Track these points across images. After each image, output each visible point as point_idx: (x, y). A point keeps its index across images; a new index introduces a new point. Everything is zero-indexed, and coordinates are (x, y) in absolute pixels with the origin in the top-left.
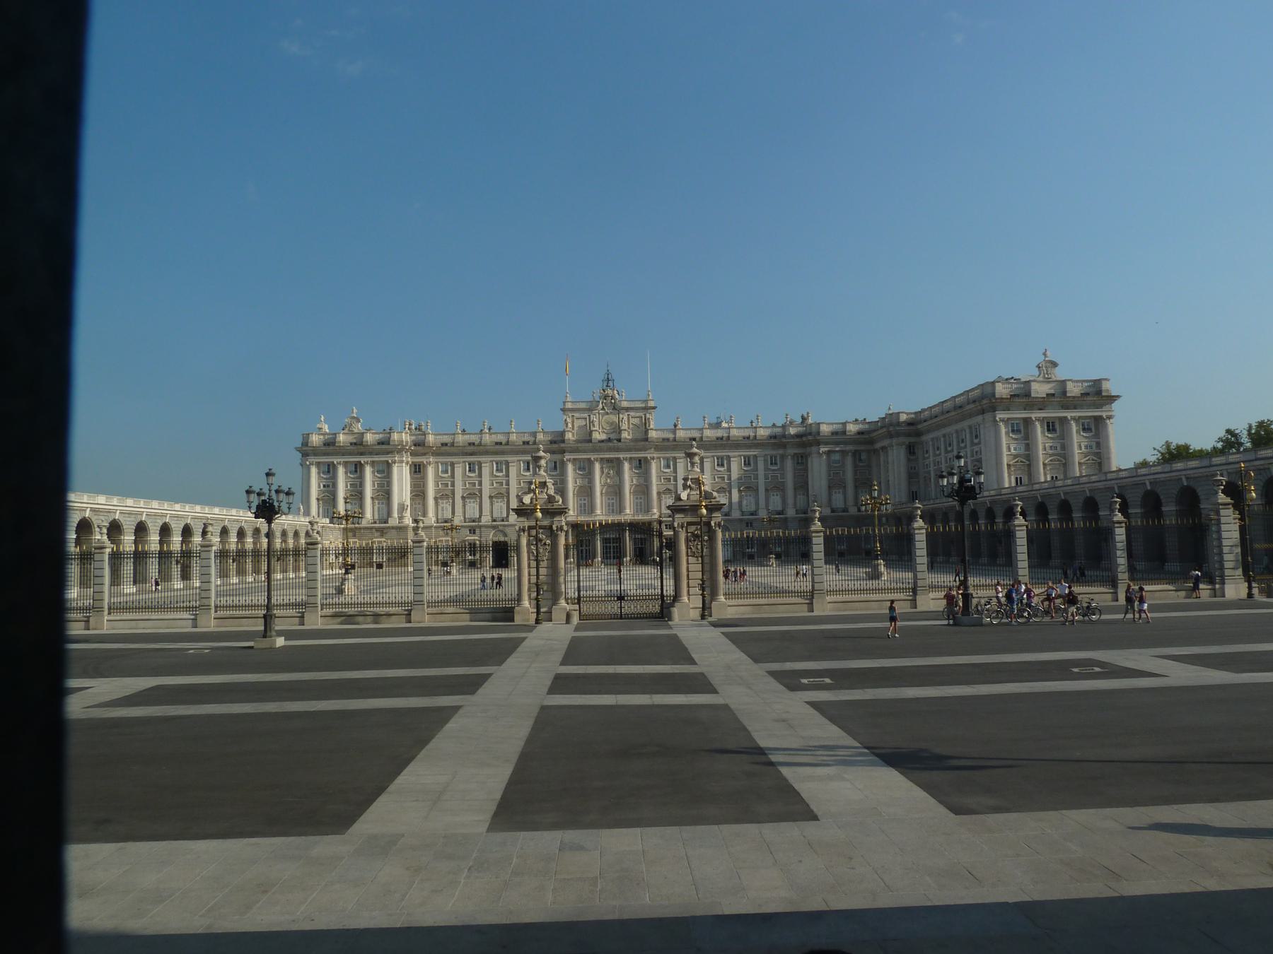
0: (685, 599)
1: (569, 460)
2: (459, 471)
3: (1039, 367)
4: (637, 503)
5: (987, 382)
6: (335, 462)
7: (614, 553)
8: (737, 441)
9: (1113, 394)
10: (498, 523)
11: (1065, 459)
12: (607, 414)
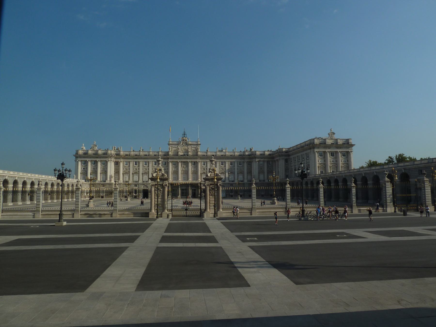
0: (208, 210)
1: (170, 162)
2: (131, 164)
3: (329, 134)
4: (193, 177)
5: (312, 139)
6: (87, 160)
8: (228, 156)
10: (145, 183)
11: (337, 165)
12: (184, 146)
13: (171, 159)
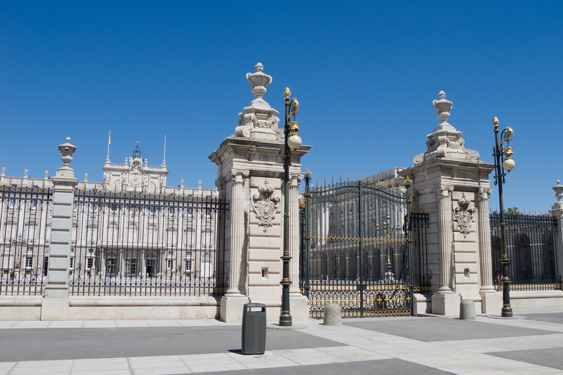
12: (135, 174)
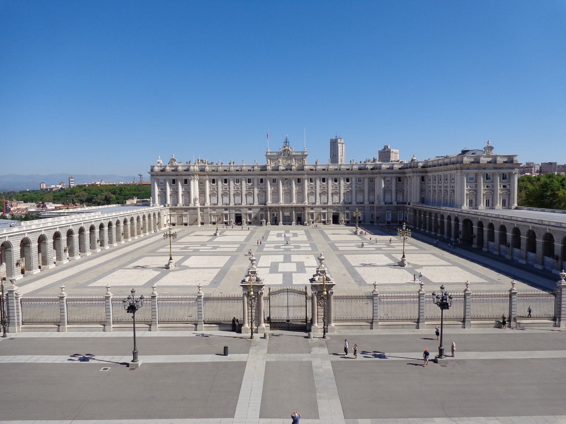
7: (288, 219)
9: (518, 163)
13: (269, 175)
